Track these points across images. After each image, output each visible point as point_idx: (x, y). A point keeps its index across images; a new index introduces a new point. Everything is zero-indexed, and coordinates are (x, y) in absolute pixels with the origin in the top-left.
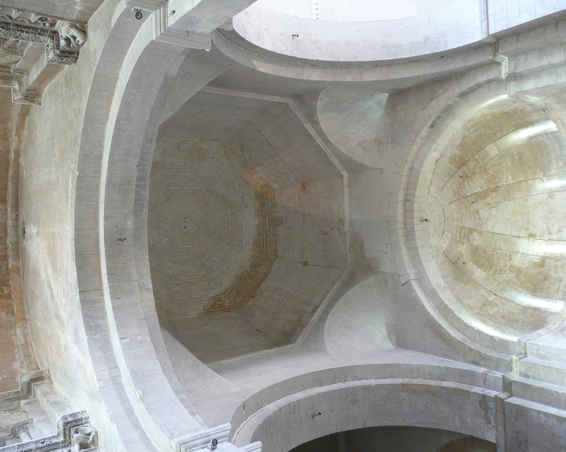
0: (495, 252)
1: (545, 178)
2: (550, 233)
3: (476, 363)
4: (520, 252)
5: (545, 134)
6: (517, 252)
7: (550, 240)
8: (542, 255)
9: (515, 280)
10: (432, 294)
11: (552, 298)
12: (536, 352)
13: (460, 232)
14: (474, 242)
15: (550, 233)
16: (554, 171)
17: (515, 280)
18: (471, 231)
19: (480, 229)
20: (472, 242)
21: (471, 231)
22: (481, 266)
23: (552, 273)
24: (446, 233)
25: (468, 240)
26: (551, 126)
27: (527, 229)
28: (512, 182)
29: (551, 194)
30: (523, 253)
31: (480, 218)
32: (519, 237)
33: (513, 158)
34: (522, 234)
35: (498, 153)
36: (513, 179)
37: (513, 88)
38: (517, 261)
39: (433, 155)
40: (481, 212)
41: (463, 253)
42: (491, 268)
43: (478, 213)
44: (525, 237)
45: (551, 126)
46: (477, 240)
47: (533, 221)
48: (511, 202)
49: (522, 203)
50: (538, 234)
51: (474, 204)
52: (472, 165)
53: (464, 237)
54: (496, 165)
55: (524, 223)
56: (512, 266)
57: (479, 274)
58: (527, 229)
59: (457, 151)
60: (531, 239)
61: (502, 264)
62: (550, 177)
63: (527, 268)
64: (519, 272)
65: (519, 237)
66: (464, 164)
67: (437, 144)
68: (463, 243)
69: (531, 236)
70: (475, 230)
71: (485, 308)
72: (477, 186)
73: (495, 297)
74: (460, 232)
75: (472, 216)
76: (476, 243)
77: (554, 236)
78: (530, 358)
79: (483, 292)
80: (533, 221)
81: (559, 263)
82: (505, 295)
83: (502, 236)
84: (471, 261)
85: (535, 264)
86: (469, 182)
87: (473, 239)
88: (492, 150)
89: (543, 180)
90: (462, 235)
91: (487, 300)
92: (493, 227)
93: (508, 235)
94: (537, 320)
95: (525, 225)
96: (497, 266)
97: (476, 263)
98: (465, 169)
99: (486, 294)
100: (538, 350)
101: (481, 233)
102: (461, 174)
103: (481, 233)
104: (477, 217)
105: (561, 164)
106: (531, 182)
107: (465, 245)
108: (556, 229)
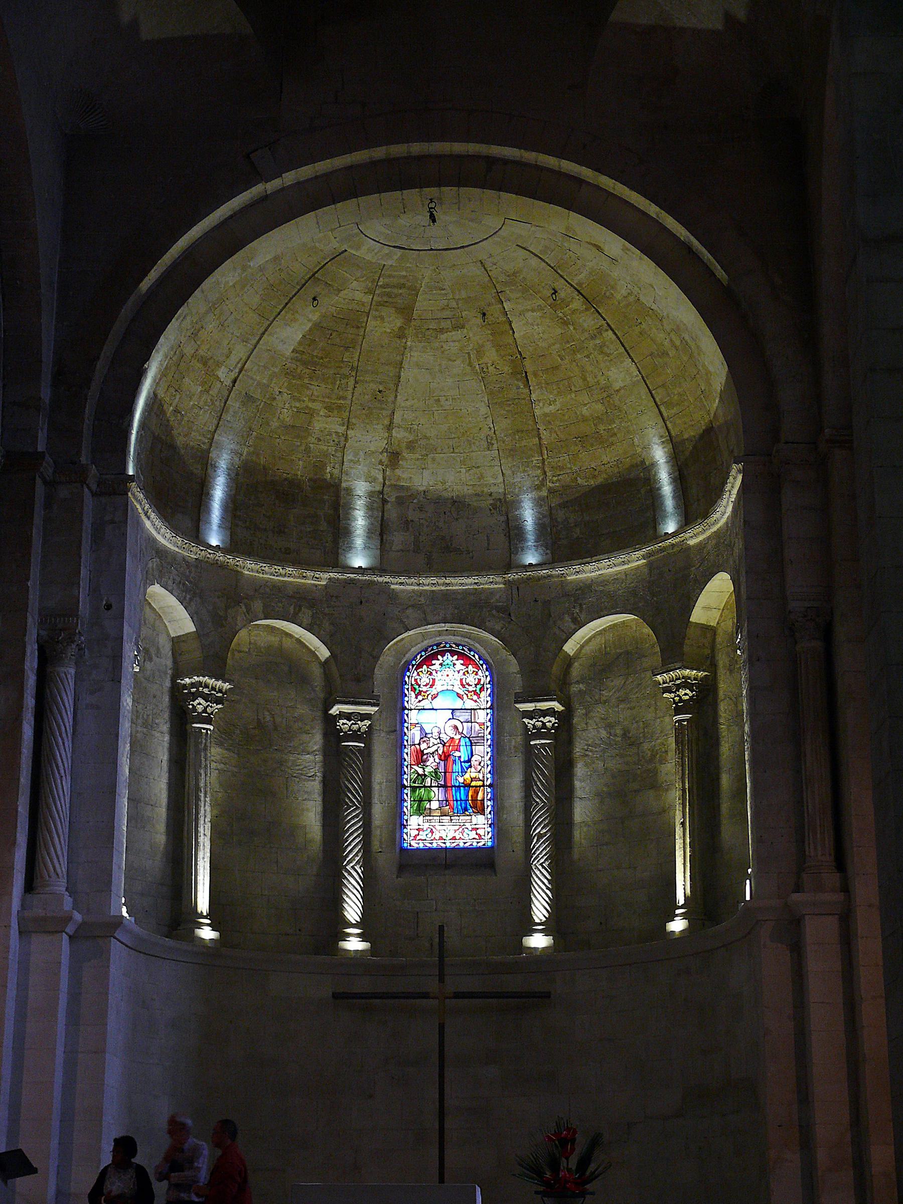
0: (346, 371)
1: (544, 493)
4: (351, 433)
5: (653, 504)
6: (349, 425)
7: (384, 501)
8: (344, 485)
9: (275, 424)
11: (234, 516)
12: (107, 518)
13: (402, 286)
14: (375, 318)
17: (275, 424)
18: (407, 312)
19: (410, 331)
20: (373, 313)
21: (407, 312)
22: (308, 340)
24: (399, 252)
25: (379, 304)
28: (537, 412)
30: (346, 439)
31: (442, 331)
32: (389, 428)
33: (599, 420)
35: (617, 386)
36: (546, 415)
40: (458, 334)
41: (342, 294)
42: (305, 363)
43: (456, 327)
44: (389, 443)
46: (381, 327)
47: (434, 459)
48: (484, 410)
49: (483, 436)
50: (398, 472)
51: (480, 320)
52: (589, 321)
53: (389, 295)
54: (585, 379)
55: (426, 437)
56: (311, 413)
57: (289, 336)
58: (411, 446)
59: (624, 292)
60: (384, 457)
61: (318, 389)
63: (308, 450)
65: (389, 428)
66: (590, 303)
67: (641, 259)
68: (371, 291)
70: (409, 319)
71: (200, 365)
73: (228, 382)
74: (402, 286)
75: (447, 313)
76: (372, 323)
79: (240, 351)
80: (434, 459)
81: (324, 526)
83: (392, 386)
84: (323, 316)
86: (540, 308)
87: (382, 318)
89: (538, 488)
90: (395, 291)
91: (218, 364)
92: (418, 366)
93: (394, 402)
95: (423, 442)
96: (311, 378)
97: (317, 326)
98: (577, 303)
99: (234, 359)
100: (112, 522)
102: (562, 294)
104: (446, 324)
107: (368, 298)
108: (412, 515)
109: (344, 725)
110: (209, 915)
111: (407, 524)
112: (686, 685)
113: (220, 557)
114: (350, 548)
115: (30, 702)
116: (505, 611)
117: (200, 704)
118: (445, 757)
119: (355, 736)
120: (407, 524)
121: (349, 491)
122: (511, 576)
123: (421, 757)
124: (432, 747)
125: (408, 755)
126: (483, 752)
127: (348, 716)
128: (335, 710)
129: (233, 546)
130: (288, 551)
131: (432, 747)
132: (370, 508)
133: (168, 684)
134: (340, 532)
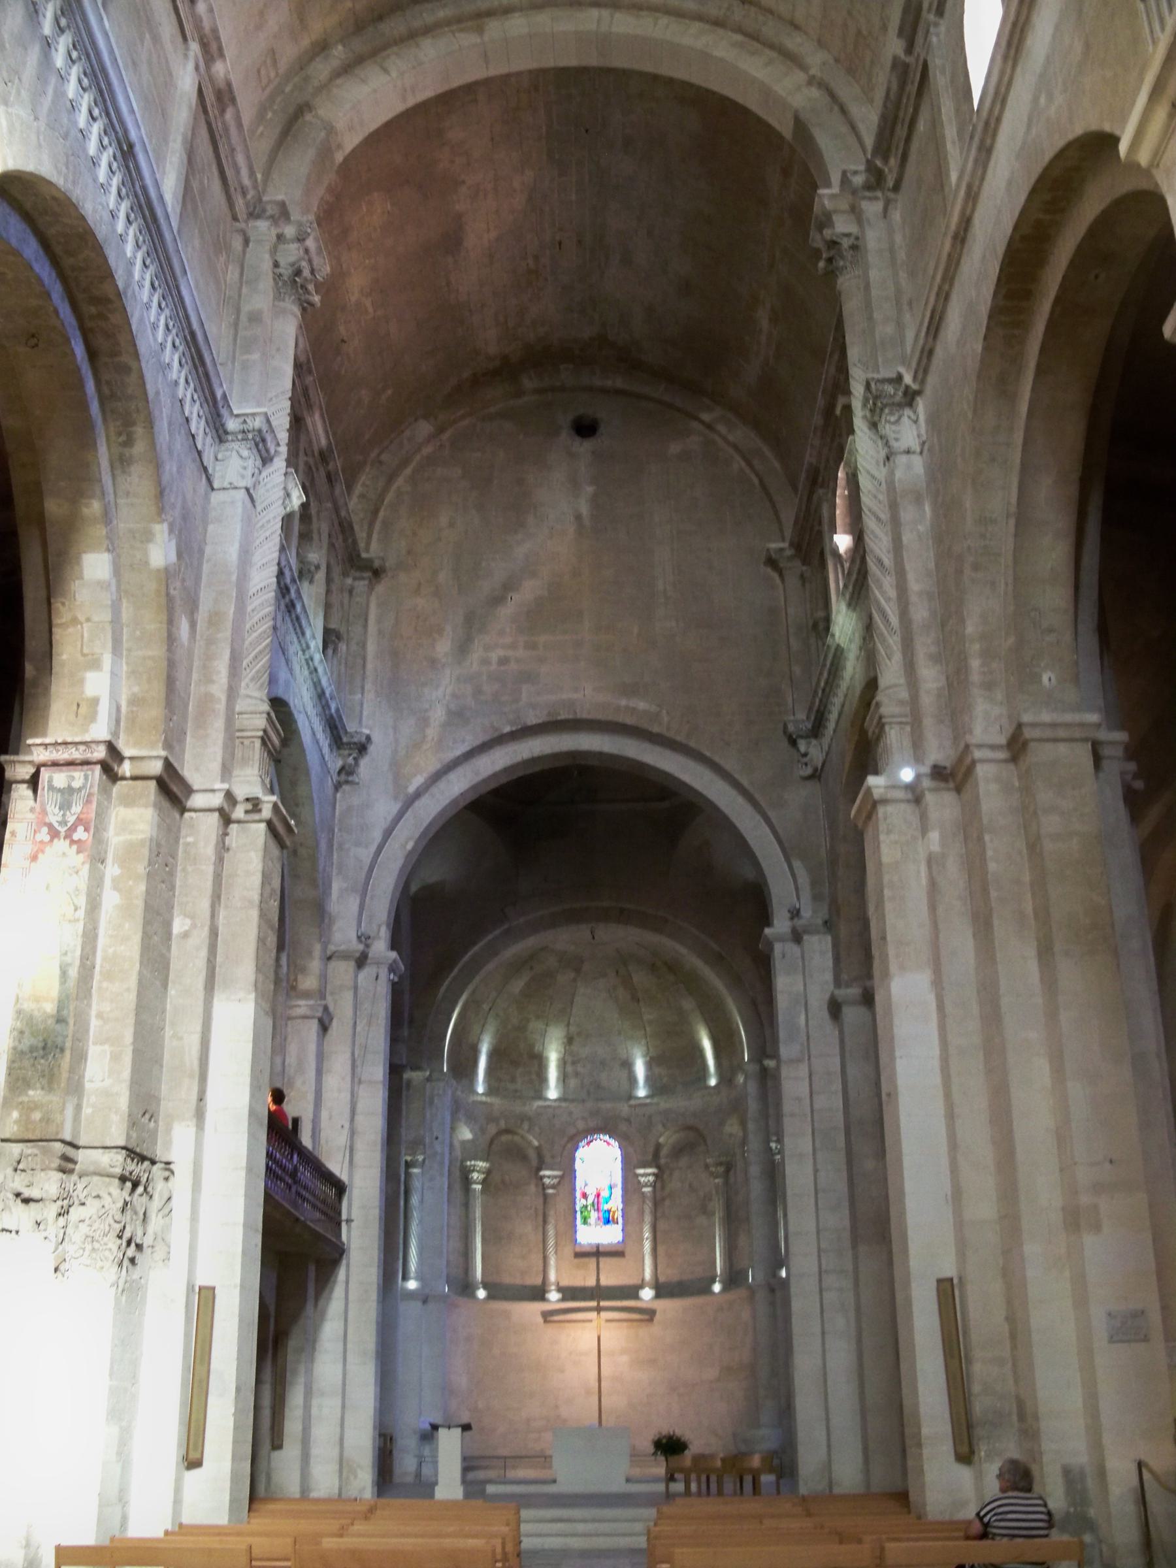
2: (574, 1063)
3: (411, 1022)
10: (493, 951)
15: (574, 1063)
16: (657, 1070)
21: (578, 970)
23: (520, 1070)
26: (713, 1082)
27: (579, 1034)
29: (628, 1065)
32: (568, 1025)
34: (573, 1029)
37: (753, 1068)
38: (535, 1025)
39: (683, 951)
45: (713, 1082)
46: (563, 978)
56: (528, 1020)
57: (517, 986)
62: (649, 1066)
64: (522, 1028)
69: (570, 1040)
72: (640, 978)
77: (569, 1069)
78: (428, 1085)
81: (534, 1077)
82: (490, 1020)
85: (532, 1047)
88: (688, 1004)
94: (464, 1068)
101: (574, 980)
103: (574, 980)
105: (665, 1080)
106: (643, 1042)
108: (580, 1069)
109: (547, 1181)
110: (482, 1282)
111: (577, 1074)
112: (721, 1164)
113: (484, 1099)
114: (547, 1087)
115: (402, 1188)
116: (628, 1120)
117: (475, 1175)
118: (598, 1195)
119: (553, 1187)
120: (577, 1074)
121: (547, 1059)
122: (632, 1102)
123: (585, 1196)
124: (591, 1192)
125: (578, 1194)
126: (618, 1192)
127: (549, 1177)
128: (542, 1173)
129: (491, 1090)
130: (516, 1091)
131: (591, 1192)
132: (558, 1067)
133: (458, 1164)
134: (542, 1079)
